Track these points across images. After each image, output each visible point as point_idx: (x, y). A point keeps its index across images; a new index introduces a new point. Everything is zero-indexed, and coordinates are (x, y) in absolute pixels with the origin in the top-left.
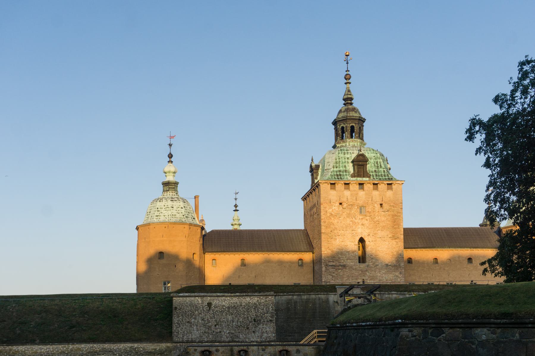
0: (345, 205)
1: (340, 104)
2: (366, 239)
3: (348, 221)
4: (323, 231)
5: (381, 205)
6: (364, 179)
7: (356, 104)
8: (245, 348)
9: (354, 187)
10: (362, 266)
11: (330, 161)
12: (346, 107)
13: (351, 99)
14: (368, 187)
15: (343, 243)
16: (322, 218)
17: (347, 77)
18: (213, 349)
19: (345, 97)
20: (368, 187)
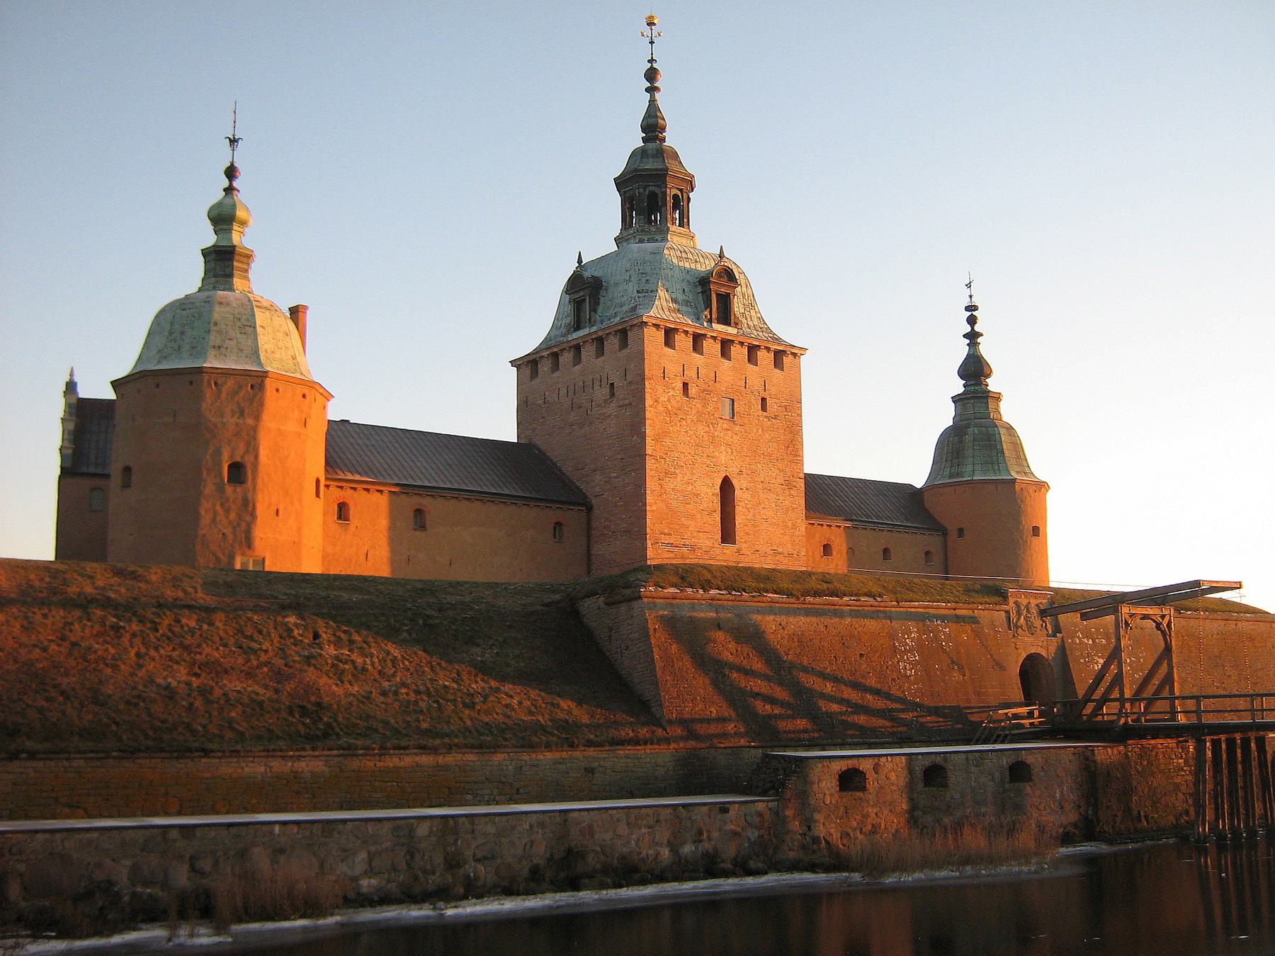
0: (693, 390)
1: (636, 140)
2: (734, 482)
3: (701, 430)
4: (649, 451)
5: (763, 399)
6: (732, 330)
7: (672, 139)
8: (939, 759)
9: (711, 347)
10: (729, 549)
11: (648, 270)
12: (651, 145)
13: (663, 129)
14: (739, 352)
15: (690, 488)
16: (648, 415)
17: (651, 75)
18: (866, 766)
19: (651, 121)
20: (739, 352)
